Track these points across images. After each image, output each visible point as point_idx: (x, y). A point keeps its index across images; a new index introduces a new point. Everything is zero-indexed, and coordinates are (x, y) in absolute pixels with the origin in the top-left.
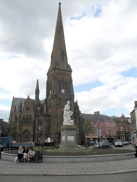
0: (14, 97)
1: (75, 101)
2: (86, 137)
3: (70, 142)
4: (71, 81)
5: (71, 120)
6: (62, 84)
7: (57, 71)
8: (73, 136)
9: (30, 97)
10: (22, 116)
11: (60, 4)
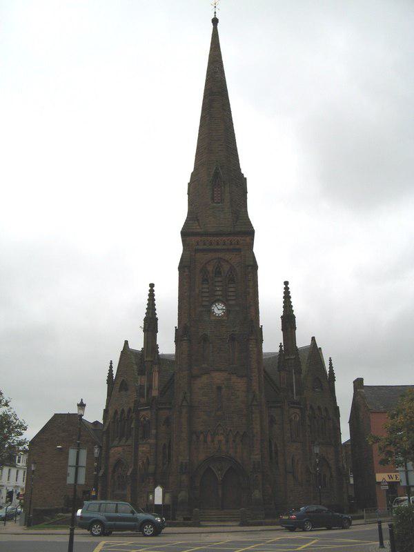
2: (380, 477)
6: (217, 284)
9: (131, 346)
11: (215, 21)
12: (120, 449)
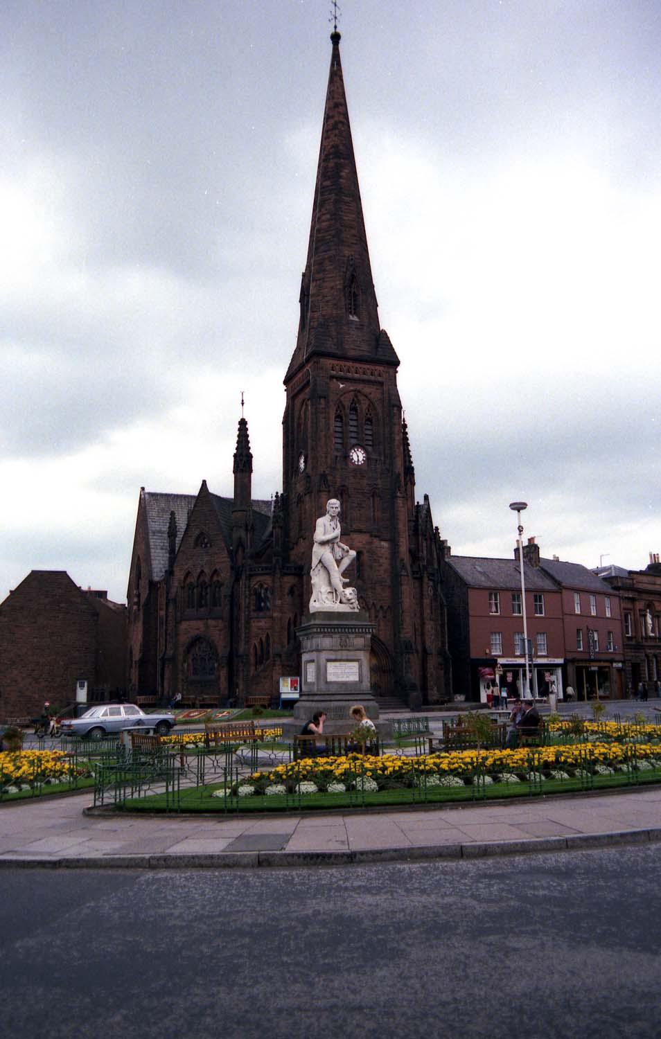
0: (143, 489)
1: (419, 499)
3: (347, 691)
4: (394, 404)
5: (345, 585)
6: (352, 423)
7: (328, 362)
8: (356, 664)
9: (212, 489)
10: (179, 575)
11: (336, 38)
12: (200, 624)
